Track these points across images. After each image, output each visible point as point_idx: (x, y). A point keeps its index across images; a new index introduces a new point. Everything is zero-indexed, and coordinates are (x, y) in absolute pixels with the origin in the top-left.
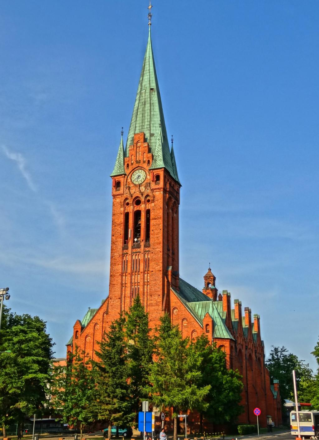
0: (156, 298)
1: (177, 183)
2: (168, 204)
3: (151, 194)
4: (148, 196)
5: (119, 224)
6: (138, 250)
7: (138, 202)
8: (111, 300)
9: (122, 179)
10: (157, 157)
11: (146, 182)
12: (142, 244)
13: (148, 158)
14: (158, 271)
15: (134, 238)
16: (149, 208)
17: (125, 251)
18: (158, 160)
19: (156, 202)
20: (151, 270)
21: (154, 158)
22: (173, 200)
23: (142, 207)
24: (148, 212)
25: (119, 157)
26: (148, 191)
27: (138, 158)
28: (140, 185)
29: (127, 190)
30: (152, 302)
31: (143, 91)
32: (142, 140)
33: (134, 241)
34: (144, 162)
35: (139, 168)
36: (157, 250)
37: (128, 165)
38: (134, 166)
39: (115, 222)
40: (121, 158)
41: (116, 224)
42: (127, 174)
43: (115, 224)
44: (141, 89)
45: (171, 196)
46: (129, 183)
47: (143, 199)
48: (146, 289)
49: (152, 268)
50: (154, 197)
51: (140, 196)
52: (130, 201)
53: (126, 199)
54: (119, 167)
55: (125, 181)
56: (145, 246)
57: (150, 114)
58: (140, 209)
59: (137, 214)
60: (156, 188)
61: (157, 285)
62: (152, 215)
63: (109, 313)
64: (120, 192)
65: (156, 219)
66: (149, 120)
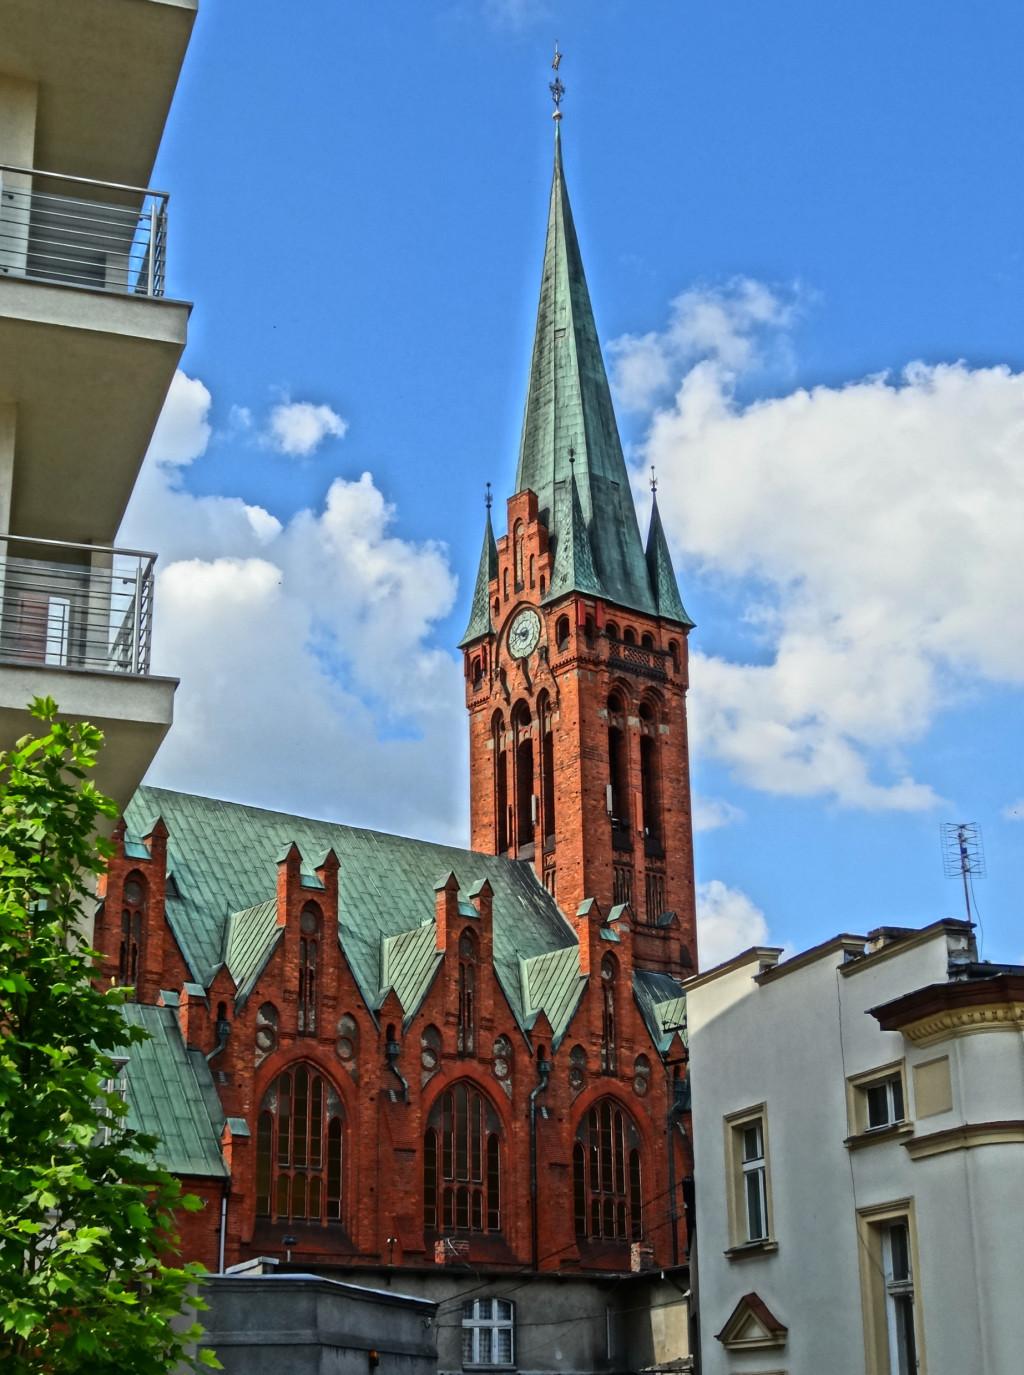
1: (663, 623)
2: (614, 704)
4: (544, 693)
7: (521, 713)
13: (541, 568)
22: (642, 684)
23: (532, 731)
24: (547, 740)
29: (497, 685)
32: (525, 515)
35: (524, 606)
37: (497, 599)
38: (513, 600)
42: (496, 630)
45: (618, 674)
47: (532, 703)
51: (525, 695)
52: (507, 717)
53: (498, 713)
59: (524, 750)
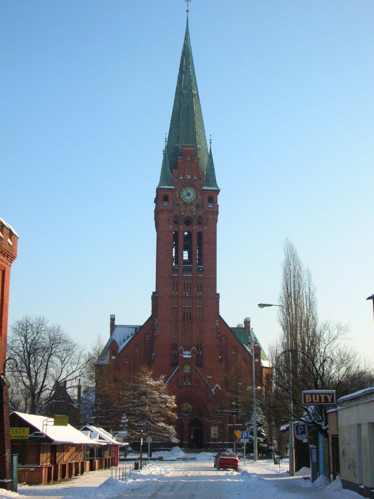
4: (200, 217)
28: (191, 204)
30: (206, 328)
40: (167, 168)
53: (176, 216)
55: (174, 196)
58: (191, 230)
65: (209, 244)
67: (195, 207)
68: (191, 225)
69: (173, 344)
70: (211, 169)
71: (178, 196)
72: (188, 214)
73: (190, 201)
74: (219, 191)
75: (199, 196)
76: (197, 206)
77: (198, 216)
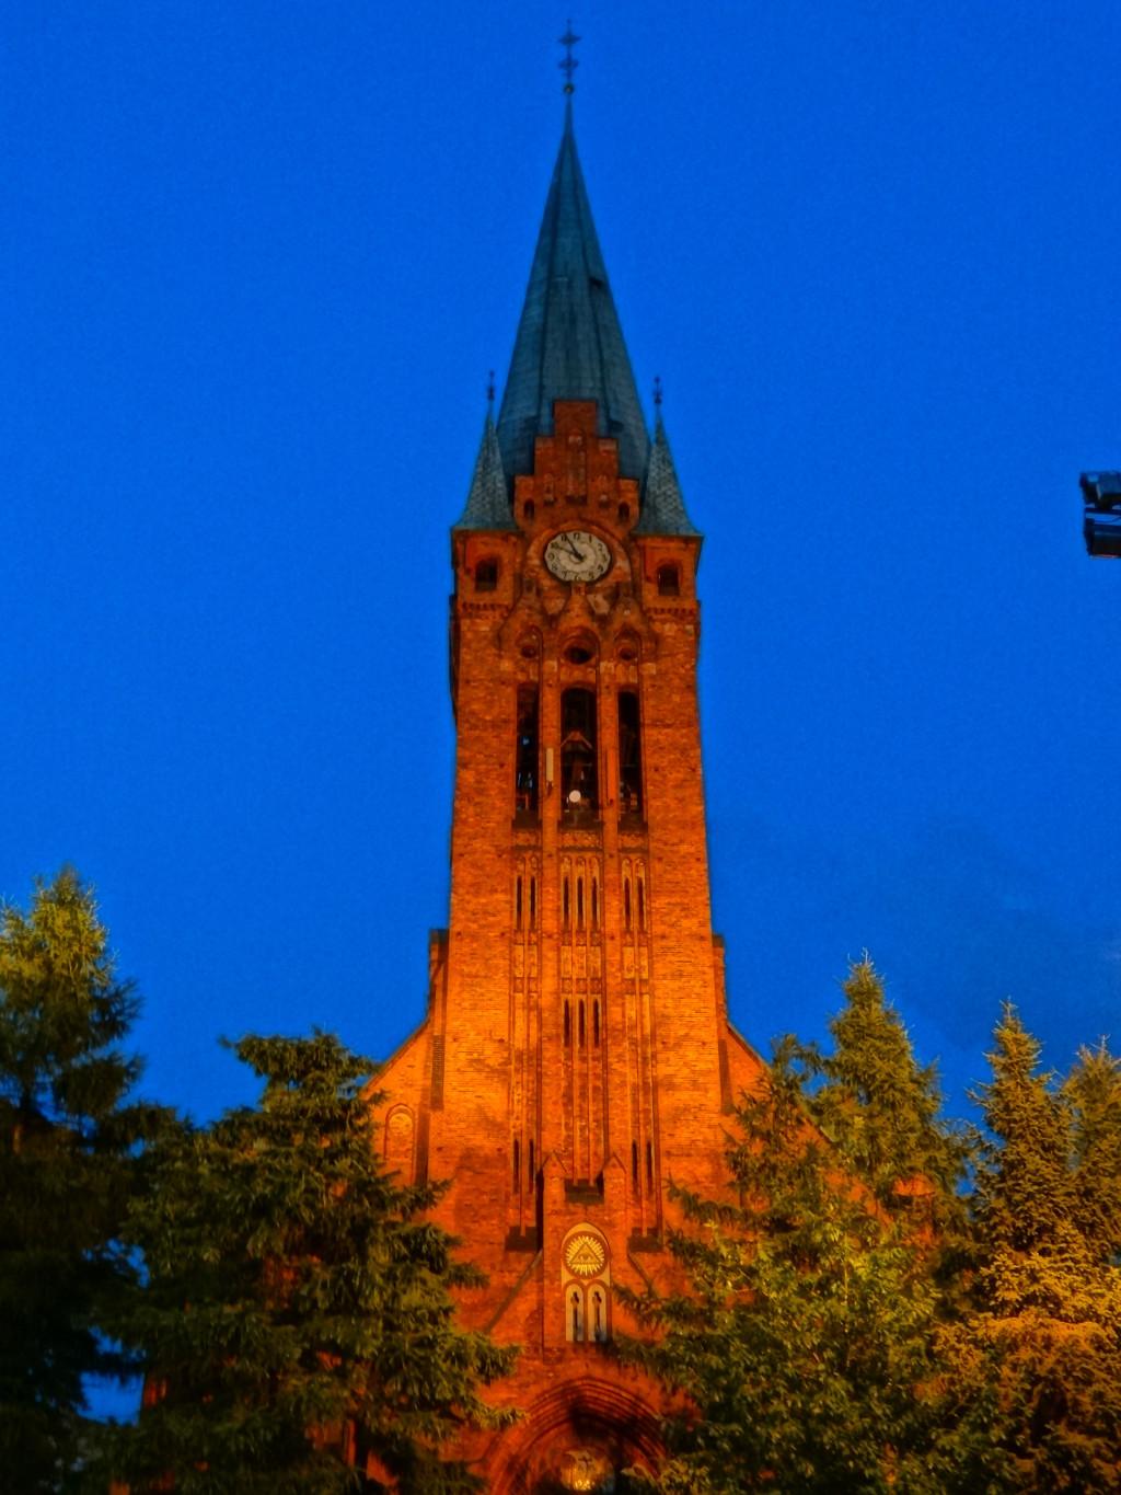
0: (691, 1055)
3: (640, 627)
4: (628, 632)
5: (494, 725)
6: (588, 839)
8: (455, 1044)
9: (506, 553)
10: (659, 500)
11: (611, 580)
12: (611, 816)
14: (691, 936)
15: (566, 791)
16: (633, 680)
17: (523, 838)
18: (664, 511)
19: (666, 663)
20: (659, 933)
21: (649, 499)
25: (484, 469)
26: (627, 613)
27: (571, 487)
28: (590, 586)
31: (560, 279)
33: (565, 804)
34: (604, 505)
36: (684, 848)
37: (529, 507)
39: (473, 713)
40: (494, 473)
41: (479, 719)
43: (473, 721)
44: (551, 272)
46: (533, 571)
48: (632, 1013)
49: (663, 923)
50: (657, 643)
54: (488, 506)
55: (518, 560)
56: (623, 826)
57: (601, 351)
58: (592, 678)
60: (667, 607)
61: (689, 996)
62: (649, 708)
63: (447, 1106)
64: (495, 595)
65: (669, 726)
66: (598, 374)
67: (605, 598)
68: (593, 661)
69: (516, 1144)
70: (663, 475)
71: (536, 562)
72: (576, 619)
73: (586, 578)
74: (699, 540)
75: (622, 564)
76: (614, 597)
77: (616, 625)
